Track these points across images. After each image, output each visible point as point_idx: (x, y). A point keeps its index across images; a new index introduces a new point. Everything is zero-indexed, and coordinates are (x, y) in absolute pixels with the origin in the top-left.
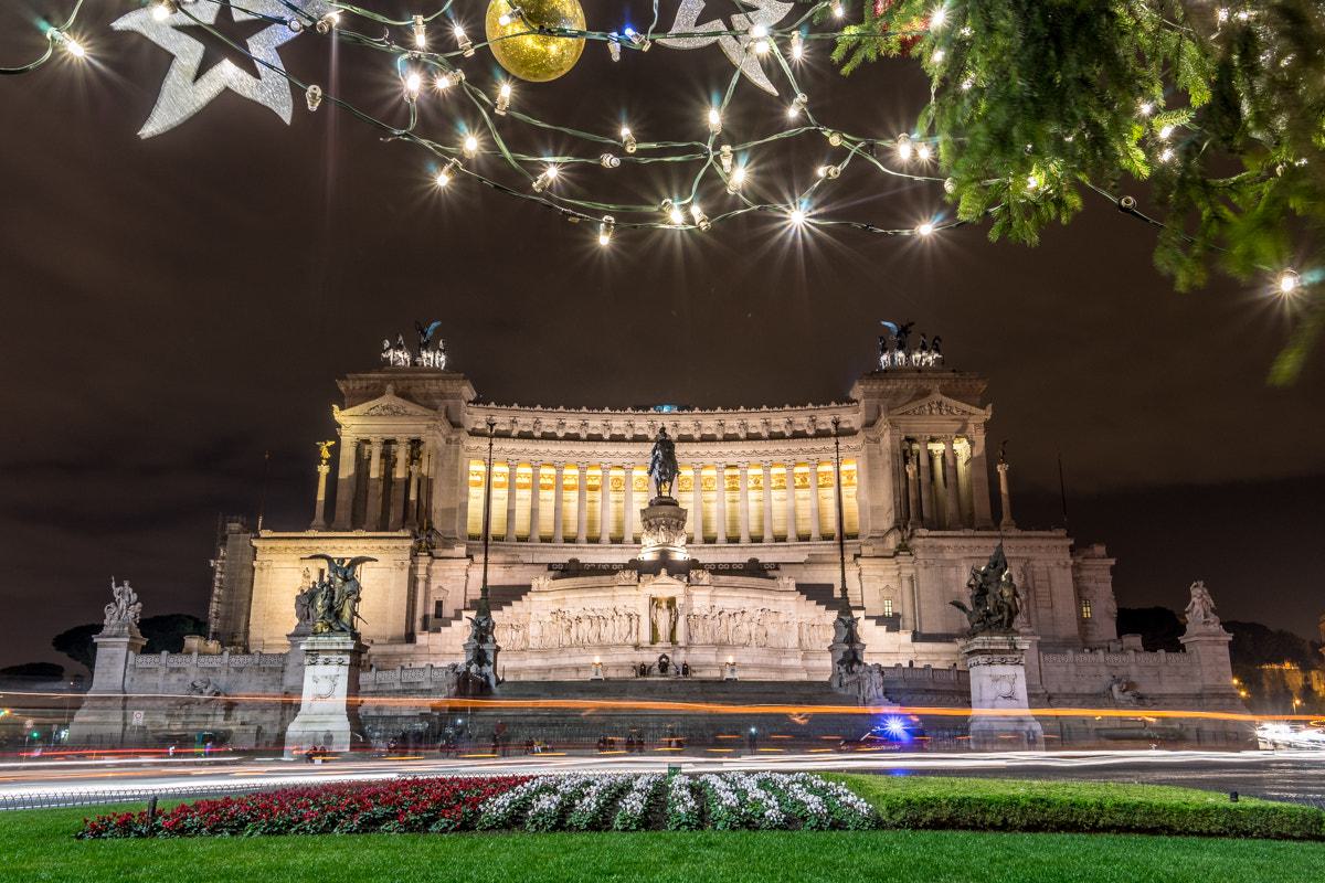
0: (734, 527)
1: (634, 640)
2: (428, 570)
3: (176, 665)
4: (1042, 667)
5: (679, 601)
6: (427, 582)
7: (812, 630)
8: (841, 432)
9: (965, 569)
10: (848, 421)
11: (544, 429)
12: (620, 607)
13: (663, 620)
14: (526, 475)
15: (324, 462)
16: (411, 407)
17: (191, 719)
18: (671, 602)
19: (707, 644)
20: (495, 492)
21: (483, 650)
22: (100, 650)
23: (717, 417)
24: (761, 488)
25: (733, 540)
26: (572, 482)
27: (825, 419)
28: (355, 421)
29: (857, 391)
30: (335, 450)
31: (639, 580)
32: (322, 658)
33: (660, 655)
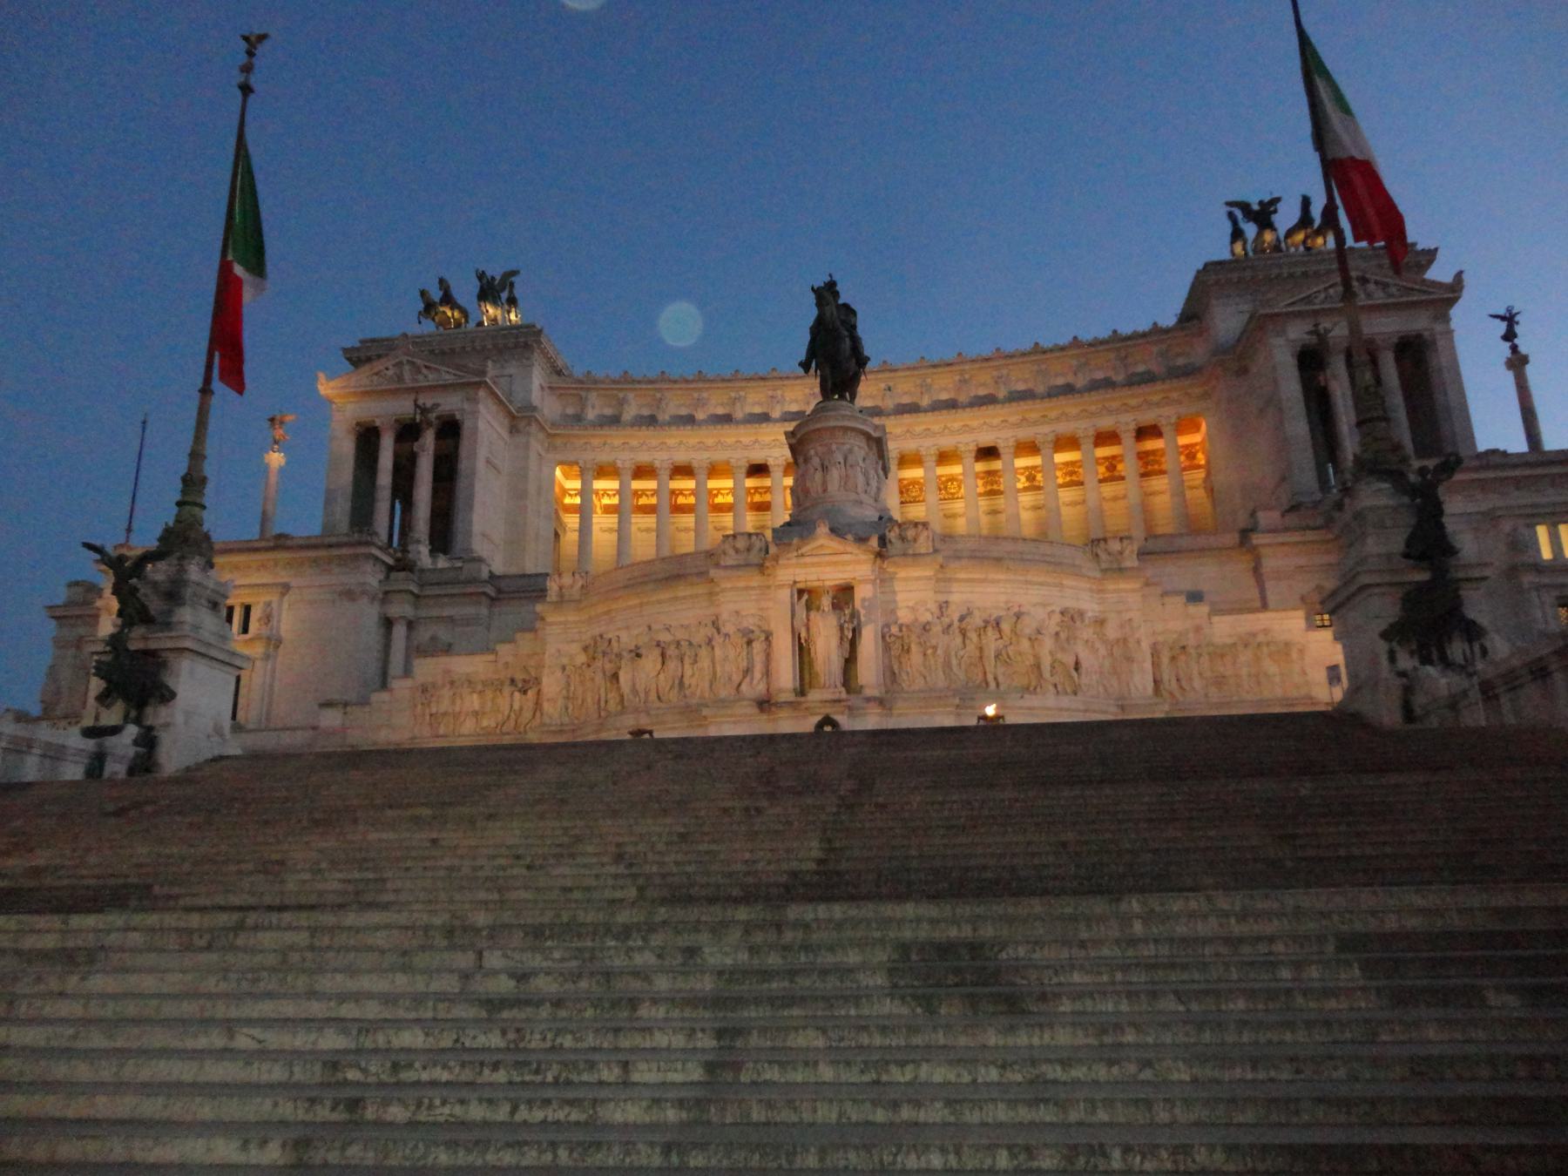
1: (760, 688)
12: (725, 612)
18: (844, 594)
24: (1039, 488)
33: (818, 718)
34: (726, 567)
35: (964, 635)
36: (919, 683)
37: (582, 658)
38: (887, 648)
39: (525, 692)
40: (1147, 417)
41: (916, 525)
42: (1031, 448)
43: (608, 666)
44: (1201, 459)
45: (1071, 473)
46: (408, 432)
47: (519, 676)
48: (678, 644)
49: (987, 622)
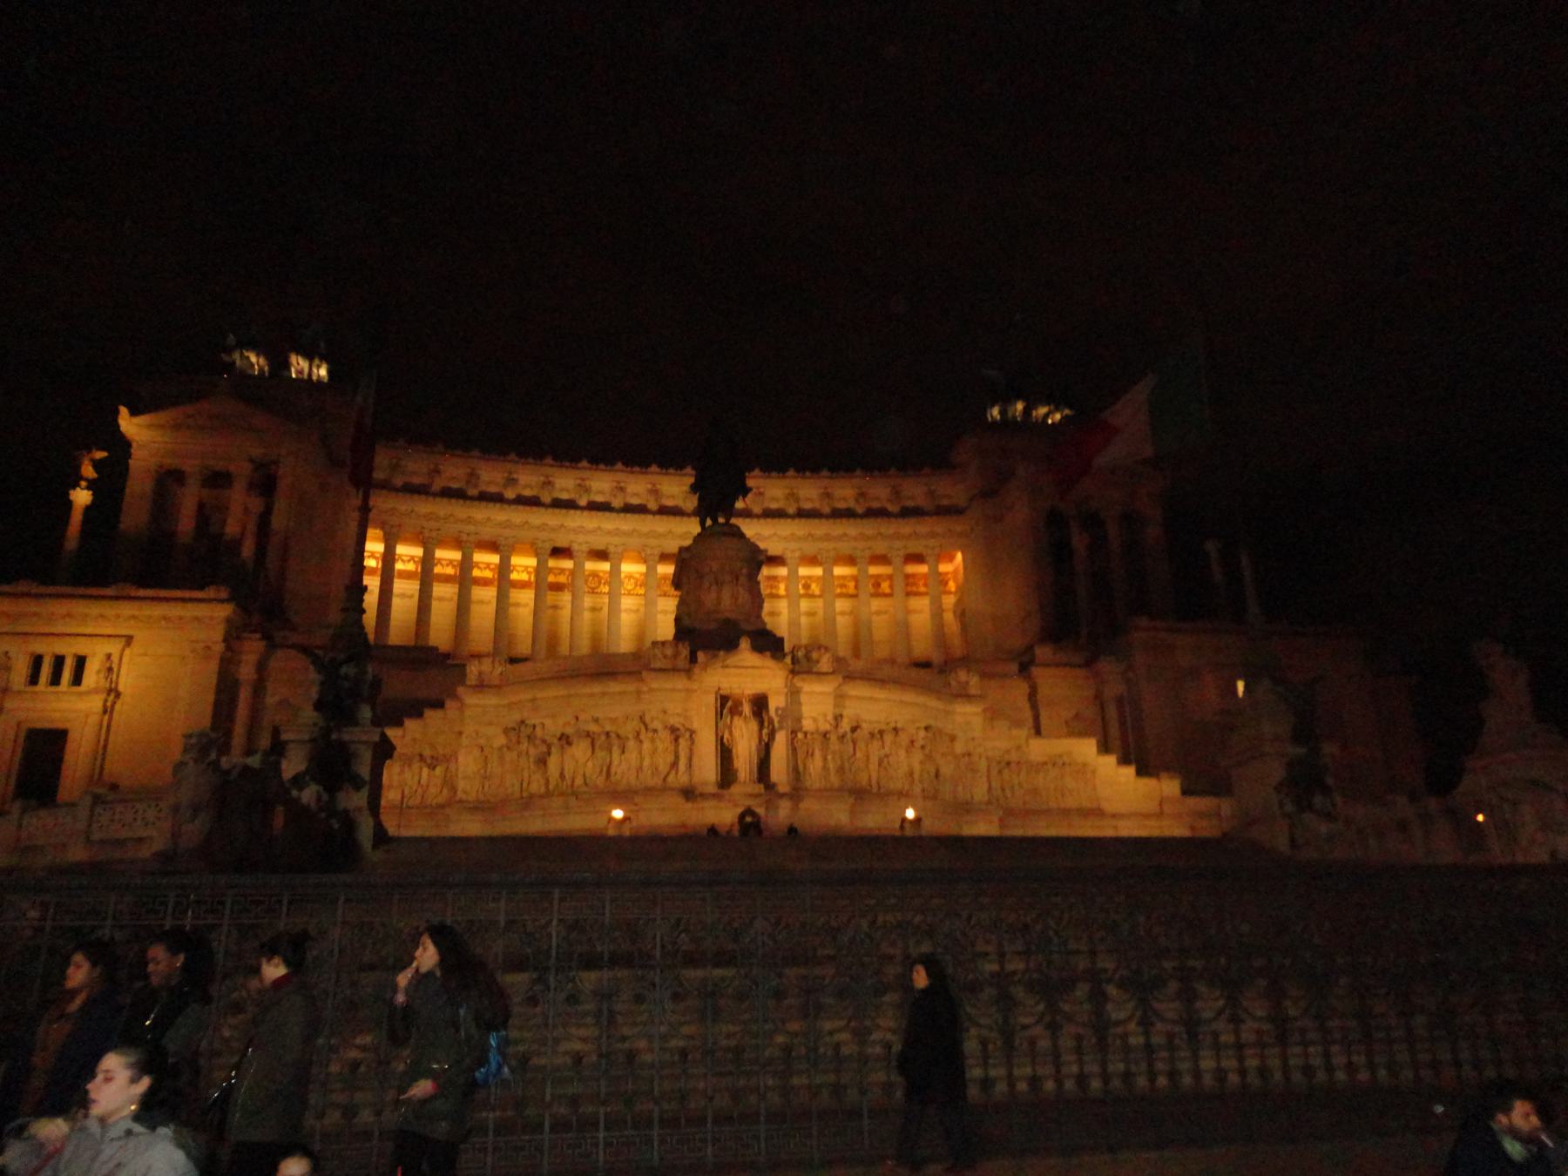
2: (261, 667)
5: (776, 703)
6: (259, 688)
7: (1006, 771)
11: (483, 488)
14: (450, 562)
15: (83, 484)
18: (760, 704)
19: (831, 789)
20: (399, 586)
21: (342, 746)
24: (813, 596)
26: (524, 577)
27: (915, 491)
31: (693, 659)
33: (740, 810)
34: (655, 670)
35: (854, 743)
36: (817, 785)
37: (501, 740)
38: (794, 750)
39: (432, 767)
40: (915, 547)
41: (819, 648)
42: (812, 561)
44: (952, 586)
45: (843, 586)
46: (218, 480)
47: (427, 752)
48: (608, 734)
49: (872, 735)
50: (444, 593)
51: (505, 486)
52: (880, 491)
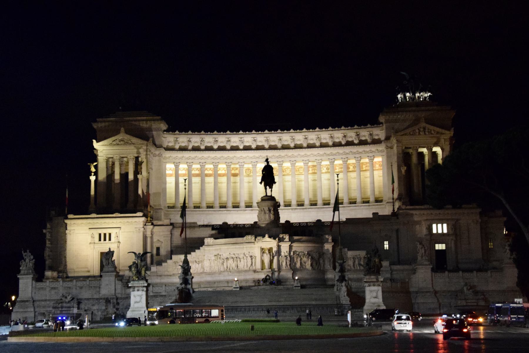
0: (315, 195)
1: (254, 268)
3: (53, 286)
4: (434, 279)
6: (152, 238)
8: (376, 142)
9: (424, 225)
10: (378, 135)
13: (267, 258)
15: (93, 174)
16: (134, 140)
17: (63, 309)
20: (181, 180)
22: (21, 281)
23: (303, 134)
25: (314, 204)
26: (223, 172)
27: (365, 133)
28: (105, 148)
29: (382, 119)
30: (96, 167)
32: (136, 289)
37: (213, 258)
39: (198, 264)
43: (221, 261)
45: (341, 168)
50: (196, 180)
51: (214, 143)
52: (351, 134)
